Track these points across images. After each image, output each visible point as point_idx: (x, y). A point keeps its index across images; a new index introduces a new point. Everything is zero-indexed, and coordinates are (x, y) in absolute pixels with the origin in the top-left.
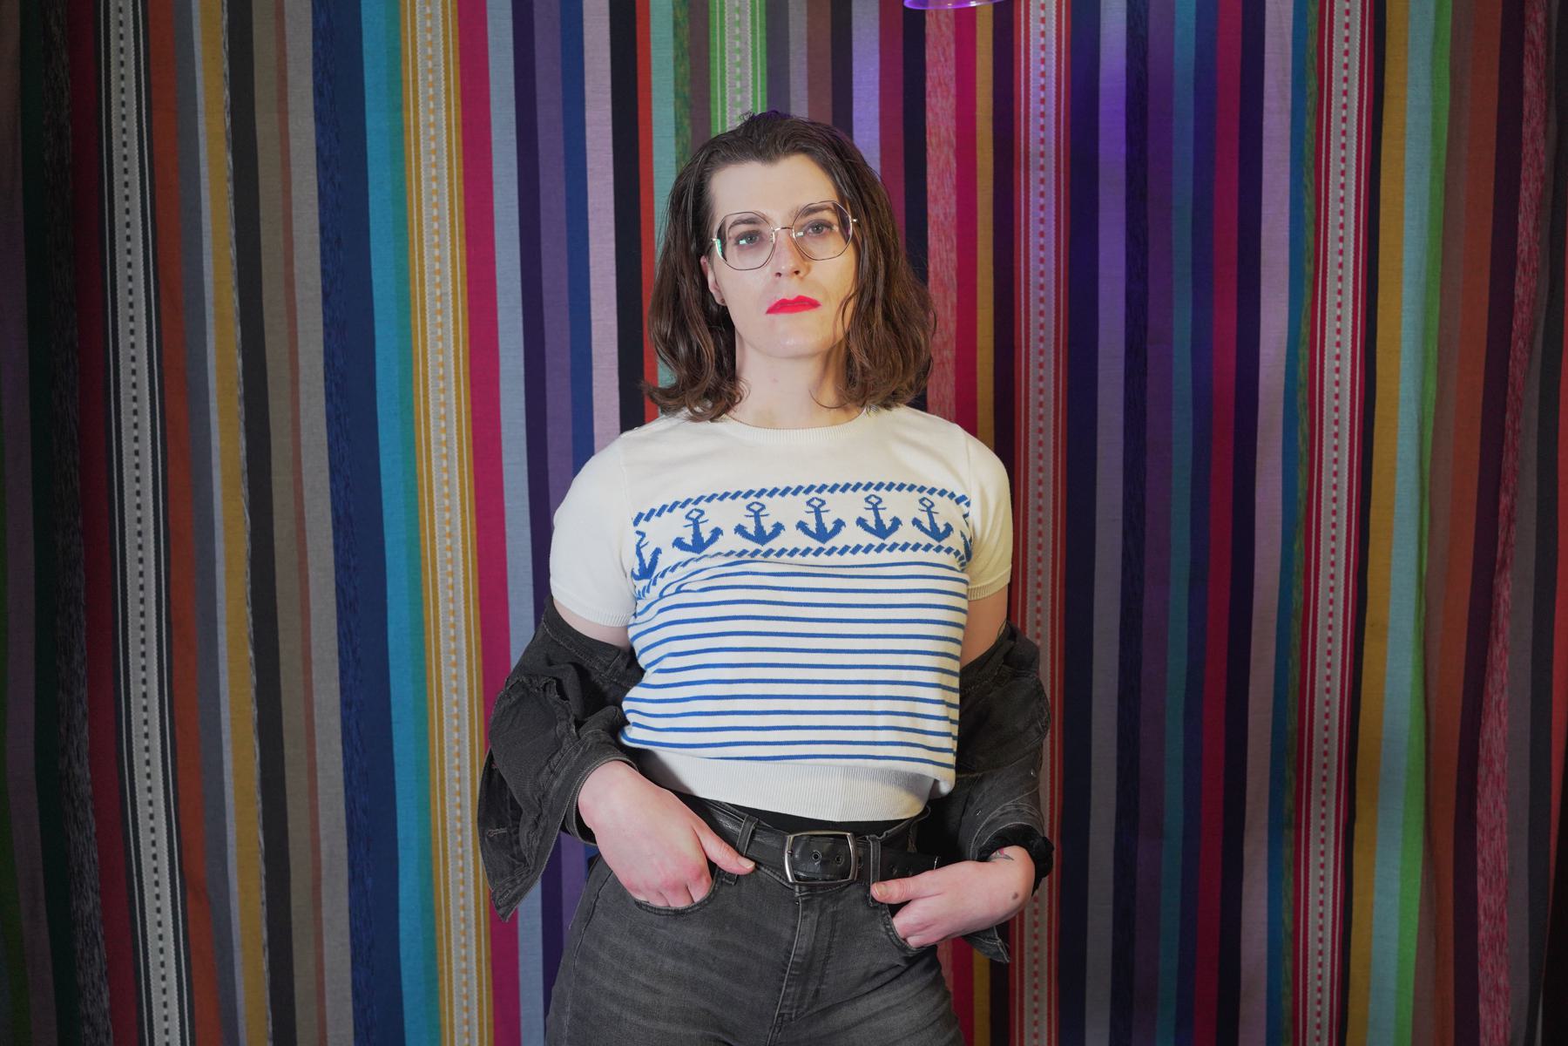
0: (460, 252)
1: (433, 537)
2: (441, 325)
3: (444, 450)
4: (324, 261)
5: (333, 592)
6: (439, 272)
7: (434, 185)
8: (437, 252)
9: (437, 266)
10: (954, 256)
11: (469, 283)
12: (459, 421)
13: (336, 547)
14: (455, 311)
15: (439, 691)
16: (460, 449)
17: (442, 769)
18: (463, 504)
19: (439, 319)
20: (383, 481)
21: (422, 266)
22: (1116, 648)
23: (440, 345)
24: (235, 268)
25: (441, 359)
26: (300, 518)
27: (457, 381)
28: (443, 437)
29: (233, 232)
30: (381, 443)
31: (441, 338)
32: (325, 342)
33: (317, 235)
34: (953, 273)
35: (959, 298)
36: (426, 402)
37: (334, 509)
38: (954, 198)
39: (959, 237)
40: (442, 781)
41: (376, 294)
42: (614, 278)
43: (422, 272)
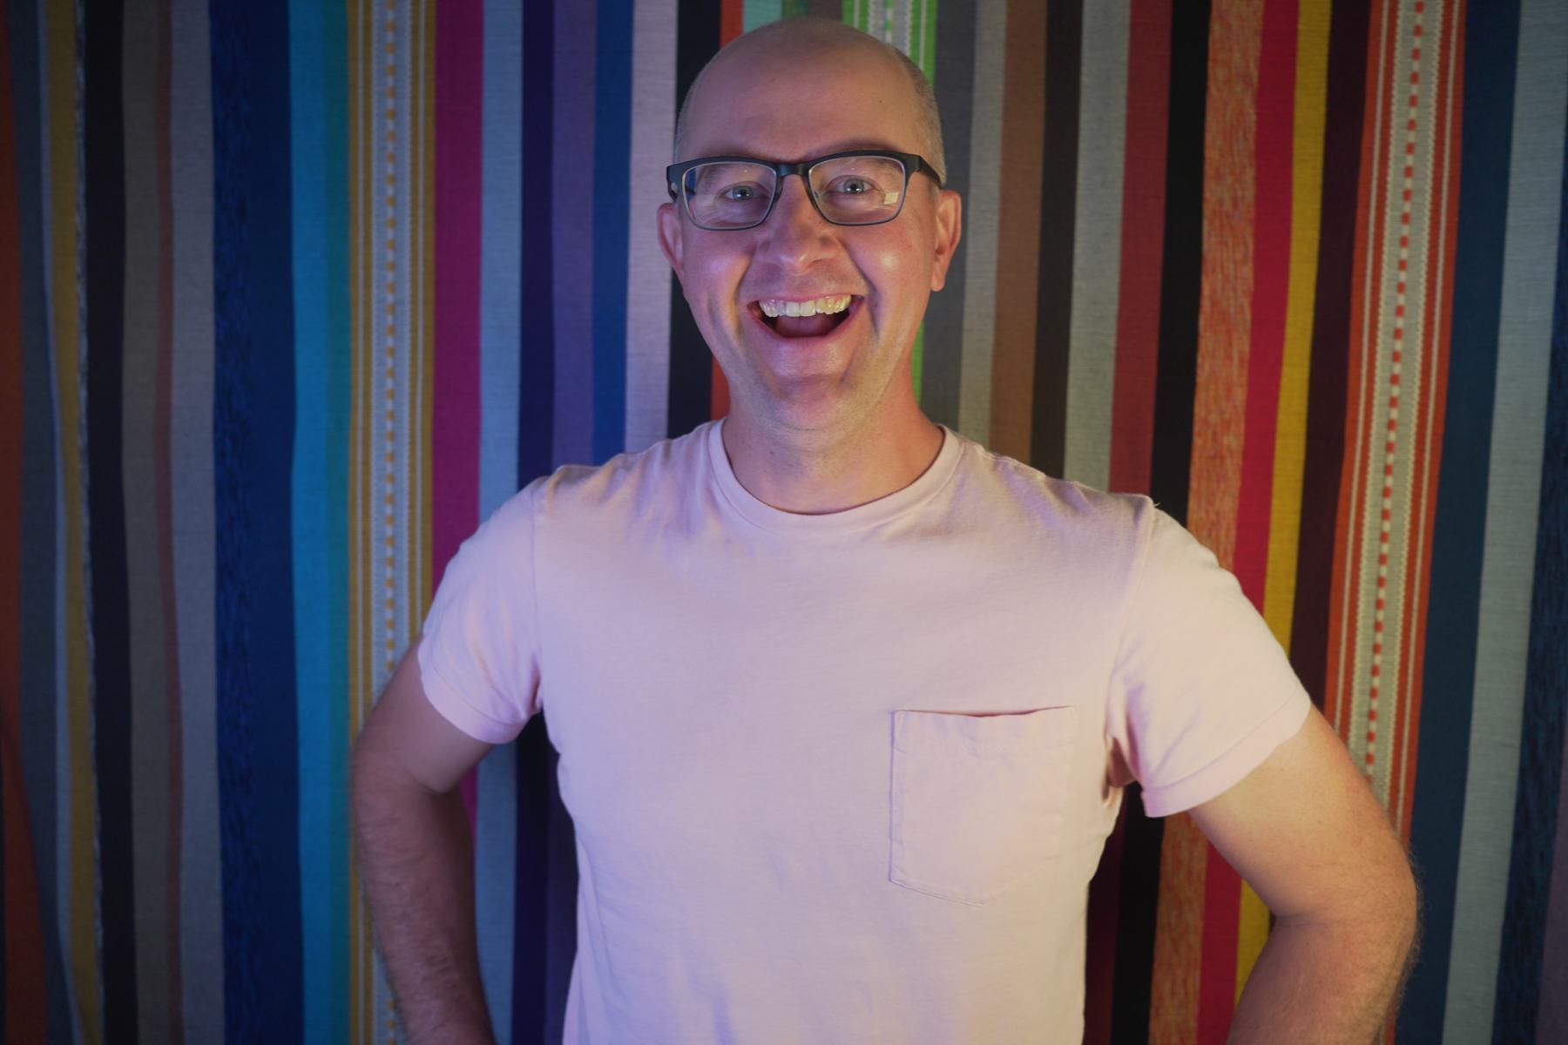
0: (425, 237)
2: (393, 352)
3: (389, 551)
4: (219, 240)
7: (390, 125)
8: (390, 234)
9: (390, 256)
10: (1248, 271)
12: (412, 506)
13: (221, 694)
14: (414, 330)
16: (412, 553)
21: (368, 256)
22: (1494, 963)
24: (82, 246)
26: (172, 644)
27: (413, 444)
29: (82, 188)
33: (209, 200)
34: (1246, 303)
35: (1255, 343)
36: (367, 473)
37: (220, 634)
38: (1250, 174)
39: (1259, 238)
43: (368, 268)
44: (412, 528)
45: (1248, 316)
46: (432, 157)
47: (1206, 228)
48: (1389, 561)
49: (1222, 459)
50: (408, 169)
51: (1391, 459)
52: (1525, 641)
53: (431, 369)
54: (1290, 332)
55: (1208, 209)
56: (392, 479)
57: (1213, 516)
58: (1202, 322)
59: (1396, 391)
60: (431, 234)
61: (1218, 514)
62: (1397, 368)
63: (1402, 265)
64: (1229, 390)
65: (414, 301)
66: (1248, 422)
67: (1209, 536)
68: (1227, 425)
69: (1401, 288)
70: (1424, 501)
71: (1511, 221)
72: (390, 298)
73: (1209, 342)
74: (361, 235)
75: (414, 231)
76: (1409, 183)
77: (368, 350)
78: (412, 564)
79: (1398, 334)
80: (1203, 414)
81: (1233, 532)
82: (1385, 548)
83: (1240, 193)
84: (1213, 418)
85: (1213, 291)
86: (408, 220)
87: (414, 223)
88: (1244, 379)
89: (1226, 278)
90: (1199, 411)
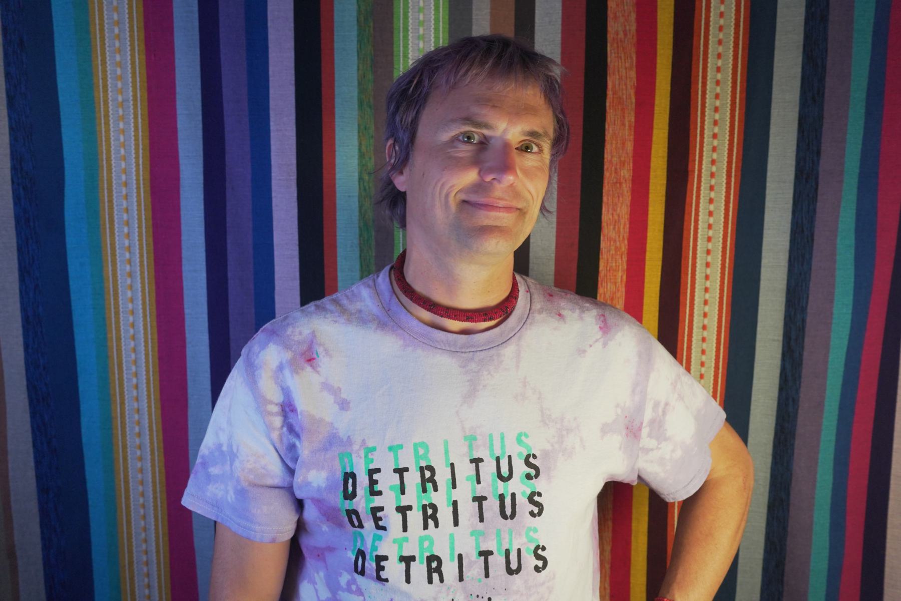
0: (140, 59)
1: (119, 339)
3: (127, 255)
5: (24, 389)
6: (120, 78)
10: (633, 74)
11: (150, 90)
12: (140, 227)
13: (26, 346)
14: (136, 117)
15: (127, 482)
16: (141, 256)
17: (130, 552)
18: (144, 309)
19: (121, 125)
20: (71, 283)
21: (105, 71)
22: (769, 460)
23: (122, 151)
25: (123, 165)
27: (138, 188)
28: (127, 242)
30: (69, 246)
31: (124, 145)
32: (12, 146)
34: (632, 92)
35: (636, 117)
36: (111, 208)
37: (24, 309)
38: (633, 16)
39: (638, 54)
40: (131, 563)
41: (61, 99)
42: (292, 89)
44: (140, 240)
45: (634, 101)
46: (141, 9)
47: (609, 49)
48: (713, 240)
49: (621, 184)
50: (127, 16)
51: (713, 182)
52: (785, 282)
53: (147, 142)
54: (657, 109)
55: (610, 37)
56: (127, 210)
57: (616, 217)
58: (607, 104)
59: (716, 143)
60: (144, 57)
61: (619, 216)
62: (716, 130)
63: (718, 69)
64: (623, 144)
65: (135, 100)
66: (635, 163)
67: (614, 228)
68: (623, 164)
69: (718, 83)
70: (731, 205)
71: (777, 43)
72: (120, 98)
73: (611, 115)
74: (100, 58)
75: (133, 56)
76: (722, 22)
77: (108, 131)
78: (141, 262)
79: (716, 110)
80: (609, 157)
81: (628, 226)
82: (711, 233)
83: (628, 28)
84: (615, 160)
85: (614, 86)
86: (129, 48)
87: (133, 50)
88: (632, 137)
89: (621, 78)
90: (607, 156)
